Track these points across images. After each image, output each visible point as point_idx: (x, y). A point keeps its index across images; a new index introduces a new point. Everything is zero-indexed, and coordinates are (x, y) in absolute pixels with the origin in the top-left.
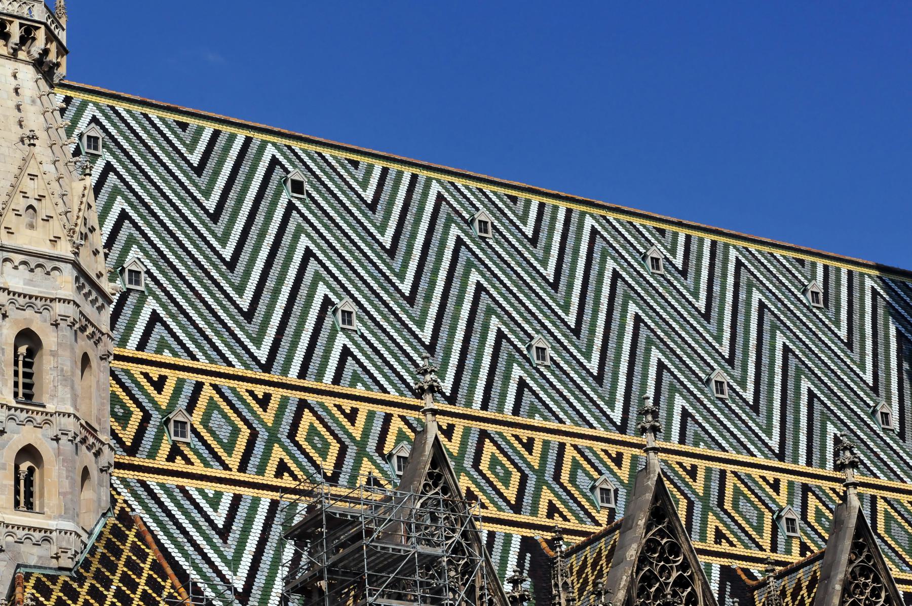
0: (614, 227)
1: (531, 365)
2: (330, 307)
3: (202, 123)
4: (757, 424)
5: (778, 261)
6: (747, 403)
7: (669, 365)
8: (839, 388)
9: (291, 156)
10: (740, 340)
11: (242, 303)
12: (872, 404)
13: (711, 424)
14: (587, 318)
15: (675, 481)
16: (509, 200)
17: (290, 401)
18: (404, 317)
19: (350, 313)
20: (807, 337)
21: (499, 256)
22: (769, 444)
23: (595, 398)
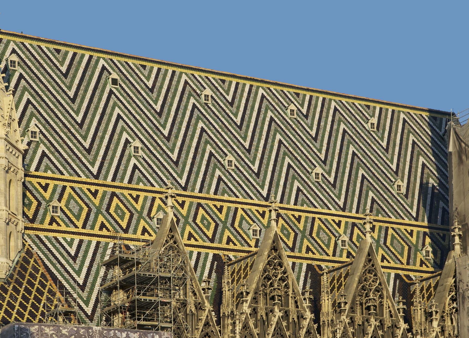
0: (273, 94)
1: (225, 169)
2: (128, 144)
3: (67, 49)
4: (334, 194)
5: (356, 107)
6: (330, 183)
7: (294, 165)
8: (378, 173)
9: (112, 65)
10: (331, 150)
11: (86, 145)
12: (393, 180)
13: (311, 195)
14: (255, 143)
15: (290, 224)
16: (221, 82)
17: (107, 193)
18: (164, 148)
19: (138, 148)
20: (366, 147)
21: (214, 113)
22: (339, 204)
23: (255, 184)
